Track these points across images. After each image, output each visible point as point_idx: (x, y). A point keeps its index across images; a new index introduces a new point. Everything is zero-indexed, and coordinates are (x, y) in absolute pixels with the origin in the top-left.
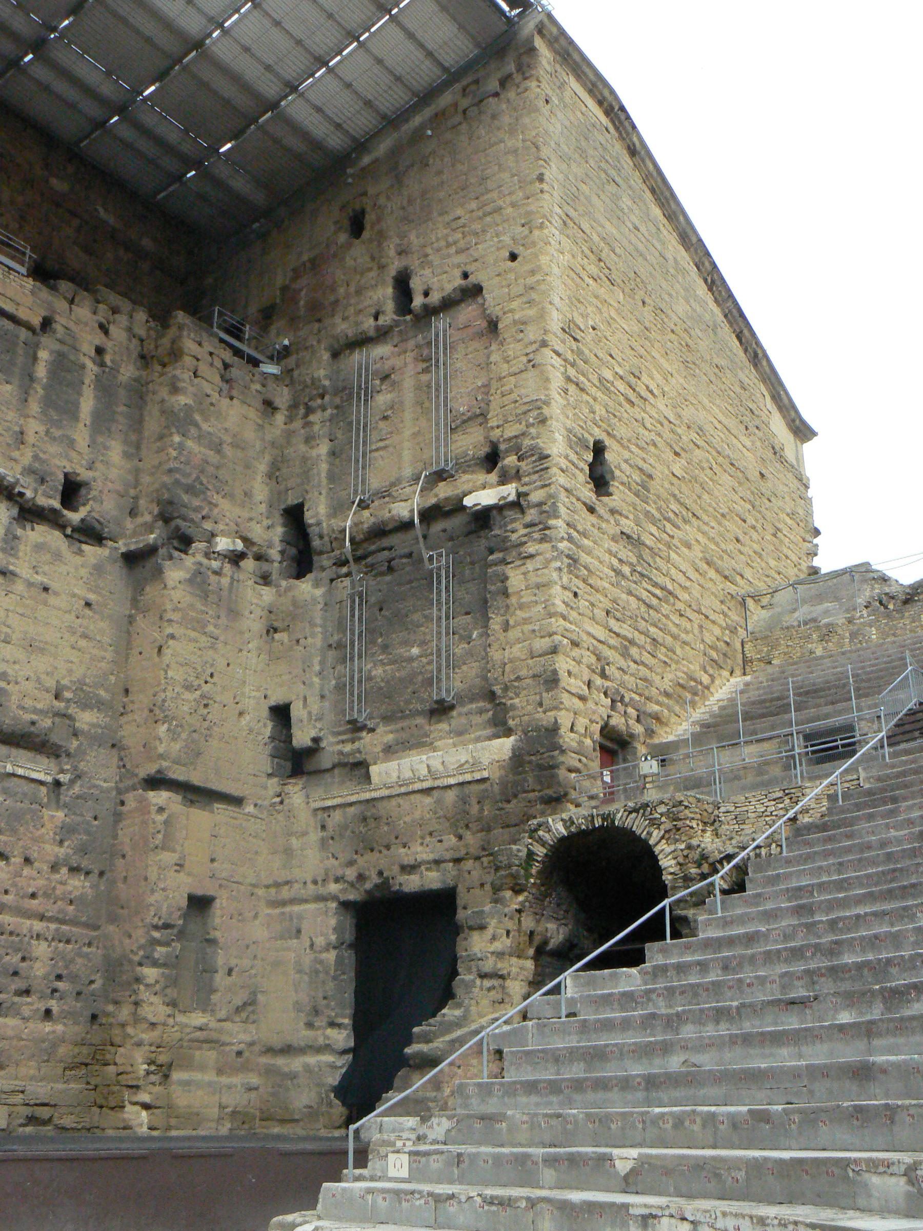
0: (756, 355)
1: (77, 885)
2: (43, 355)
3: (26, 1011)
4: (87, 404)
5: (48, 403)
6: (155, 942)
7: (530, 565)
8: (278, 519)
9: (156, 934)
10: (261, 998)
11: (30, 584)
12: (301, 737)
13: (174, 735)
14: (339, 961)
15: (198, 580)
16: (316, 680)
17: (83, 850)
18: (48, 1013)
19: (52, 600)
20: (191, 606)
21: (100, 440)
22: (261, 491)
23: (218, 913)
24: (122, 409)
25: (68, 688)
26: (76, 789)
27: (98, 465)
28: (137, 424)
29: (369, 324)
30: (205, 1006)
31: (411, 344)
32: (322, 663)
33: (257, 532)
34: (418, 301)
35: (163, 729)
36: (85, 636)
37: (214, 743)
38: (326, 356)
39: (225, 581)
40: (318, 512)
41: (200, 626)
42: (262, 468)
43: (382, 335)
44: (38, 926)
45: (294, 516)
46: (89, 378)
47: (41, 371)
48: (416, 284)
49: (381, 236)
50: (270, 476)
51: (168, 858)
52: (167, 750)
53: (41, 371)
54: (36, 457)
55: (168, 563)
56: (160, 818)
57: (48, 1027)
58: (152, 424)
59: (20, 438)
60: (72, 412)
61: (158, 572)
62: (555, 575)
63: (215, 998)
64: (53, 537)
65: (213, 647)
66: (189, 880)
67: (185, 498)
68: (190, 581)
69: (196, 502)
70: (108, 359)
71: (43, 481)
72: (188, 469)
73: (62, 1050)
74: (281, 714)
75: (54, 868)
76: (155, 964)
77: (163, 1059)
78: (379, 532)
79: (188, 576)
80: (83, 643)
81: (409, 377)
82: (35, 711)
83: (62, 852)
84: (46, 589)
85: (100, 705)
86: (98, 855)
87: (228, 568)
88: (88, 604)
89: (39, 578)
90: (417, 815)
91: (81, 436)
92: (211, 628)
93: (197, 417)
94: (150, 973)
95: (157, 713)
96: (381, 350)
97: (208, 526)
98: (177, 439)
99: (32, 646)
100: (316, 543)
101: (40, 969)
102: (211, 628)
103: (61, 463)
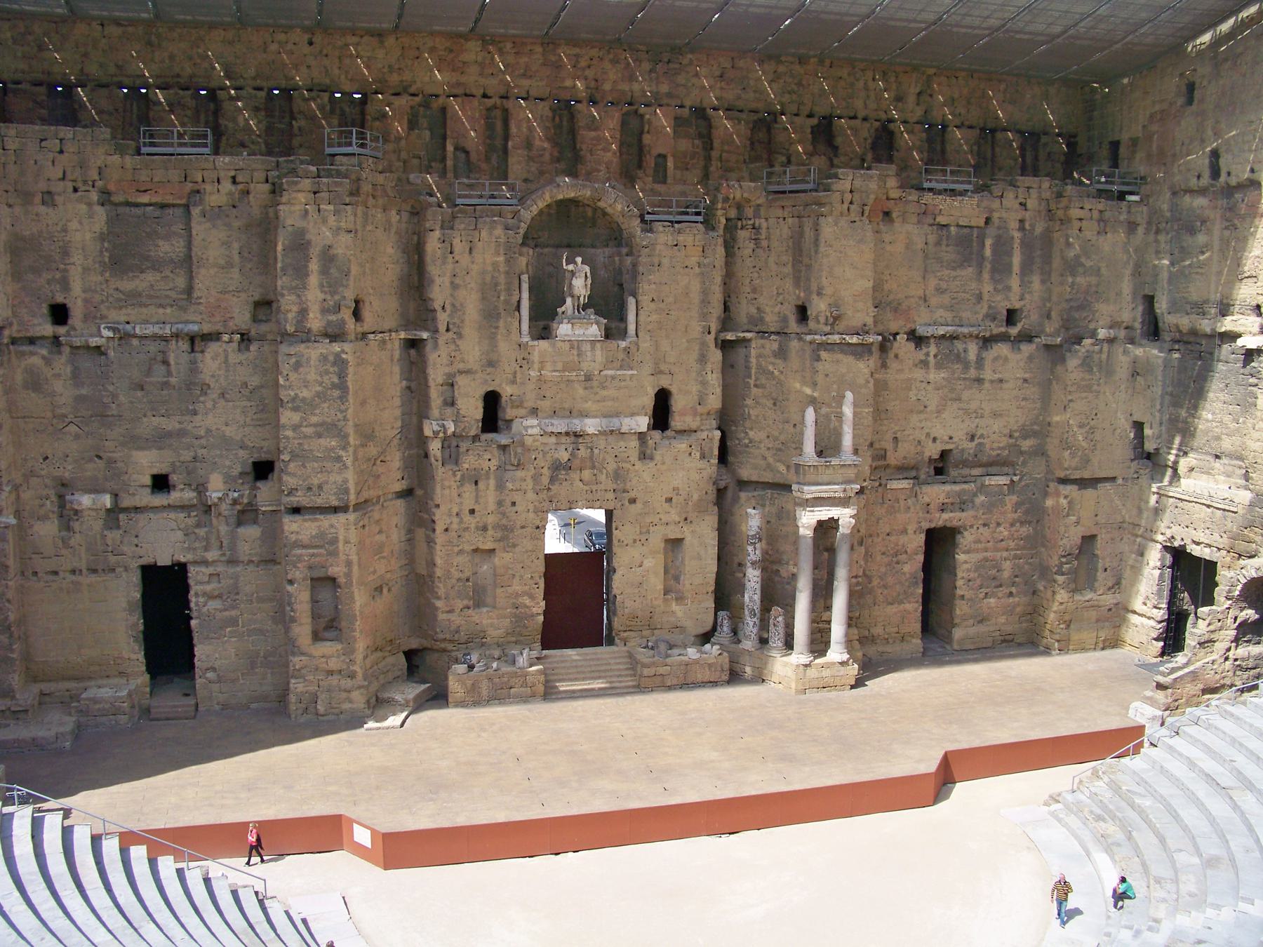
1: (1025, 530)
2: (988, 242)
3: (1000, 595)
4: (1016, 260)
5: (994, 271)
6: (1062, 563)
8: (1140, 300)
9: (1064, 560)
10: (1123, 582)
11: (992, 382)
12: (1150, 446)
13: (1073, 455)
14: (1161, 576)
15: (1087, 364)
16: (1157, 414)
17: (1027, 512)
18: (1011, 594)
19: (1005, 386)
20: (1083, 379)
22: (1126, 287)
24: (1039, 252)
27: (1027, 296)
28: (1047, 259)
29: (1193, 183)
30: (1093, 589)
31: (1220, 202)
32: (1162, 404)
33: (1126, 316)
34: (1223, 178)
35: (1067, 453)
36: (1024, 399)
38: (1168, 195)
39: (1104, 356)
40: (1161, 306)
41: (1088, 388)
42: (1128, 272)
43: (1202, 192)
44: (1005, 554)
45: (1150, 300)
46: (1016, 245)
47: (988, 252)
48: (1222, 162)
49: (1202, 101)
50: (1133, 275)
52: (1068, 463)
53: (988, 252)
54: (990, 307)
55: (1068, 354)
57: (1011, 600)
58: (1056, 263)
59: (980, 297)
60: (1008, 269)
61: (1063, 360)
63: (1096, 584)
64: (1002, 349)
67: (1077, 315)
68: (1082, 365)
70: (1027, 227)
71: (995, 319)
73: (1018, 609)
75: (1012, 525)
76: (1063, 574)
77: (1067, 617)
78: (1194, 332)
80: (1023, 403)
81: (1217, 228)
82: (999, 448)
83: (1016, 516)
84: (1001, 381)
85: (1035, 434)
86: (1034, 514)
87: (1106, 346)
88: (1025, 380)
89: (997, 376)
90: (1202, 515)
91: (1015, 282)
93: (1083, 260)
94: (1060, 579)
95: (1066, 445)
96: (1200, 201)
97: (1092, 326)
98: (1070, 280)
99: (996, 415)
100: (1160, 325)
101: (1006, 574)
102: (1095, 387)
103: (1003, 306)
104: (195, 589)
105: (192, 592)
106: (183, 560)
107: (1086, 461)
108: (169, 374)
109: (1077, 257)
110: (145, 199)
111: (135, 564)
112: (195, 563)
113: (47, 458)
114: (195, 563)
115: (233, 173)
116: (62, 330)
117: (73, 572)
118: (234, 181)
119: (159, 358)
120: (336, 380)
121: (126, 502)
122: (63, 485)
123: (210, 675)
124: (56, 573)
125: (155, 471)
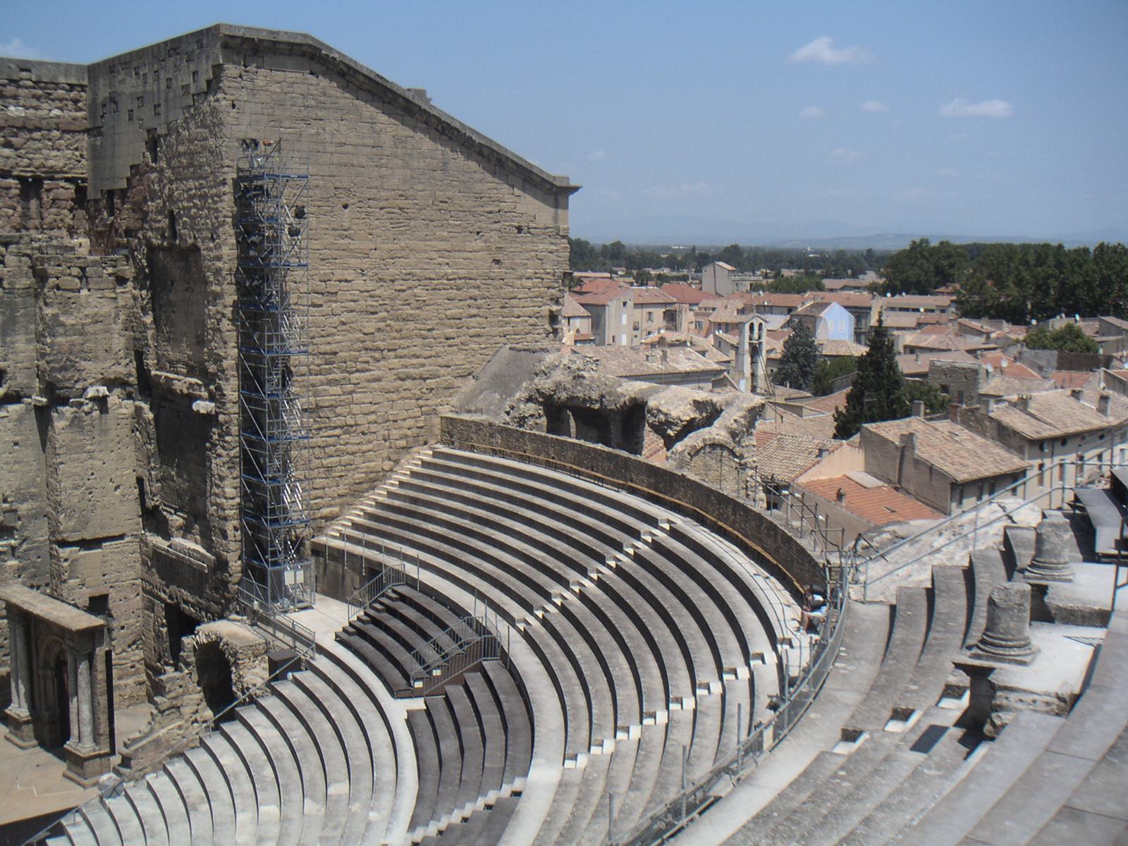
0: (499, 160)
7: (218, 461)
15: (76, 423)
20: (72, 440)
21: (8, 339)
22: (119, 342)
23: (110, 601)
25: (9, 496)
26: (24, 546)
27: (10, 356)
36: (16, 462)
37: (98, 512)
41: (80, 449)
51: (72, 582)
56: (66, 564)
62: (228, 472)
65: (91, 458)
66: (89, 590)
68: (70, 426)
69: (69, 375)
72: (59, 356)
74: (140, 481)
79: (67, 423)
80: (16, 467)
88: (16, 444)
92: (89, 447)
93: (62, 319)
98: (49, 340)
107: (85, 523)
109: (55, 316)
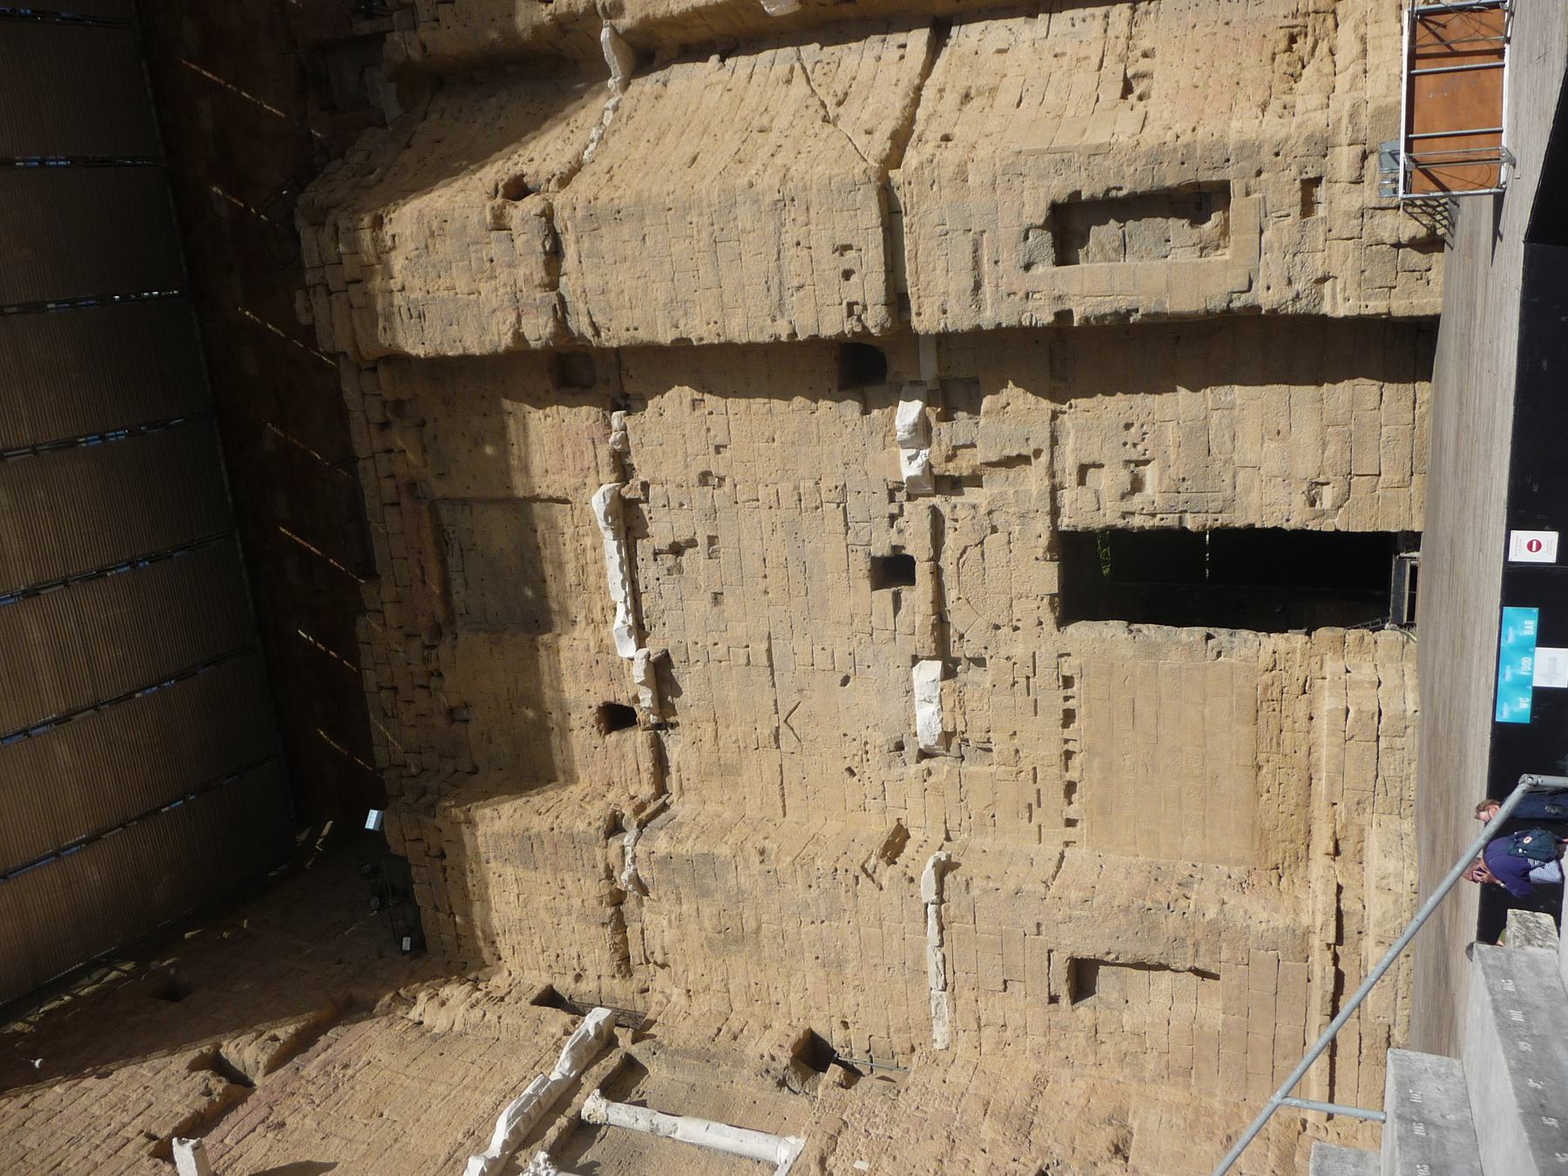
104: (1109, 516)
105: (1121, 523)
106: (1044, 541)
108: (692, 543)
110: (433, 569)
111: (1052, 640)
112: (1055, 512)
113: (851, 771)
114: (1055, 512)
115: (373, 429)
116: (640, 716)
117: (1068, 755)
118: (385, 426)
119: (669, 560)
120: (626, 231)
121: (927, 643)
122: (900, 747)
123: (1328, 497)
124: (1070, 788)
125: (867, 584)
